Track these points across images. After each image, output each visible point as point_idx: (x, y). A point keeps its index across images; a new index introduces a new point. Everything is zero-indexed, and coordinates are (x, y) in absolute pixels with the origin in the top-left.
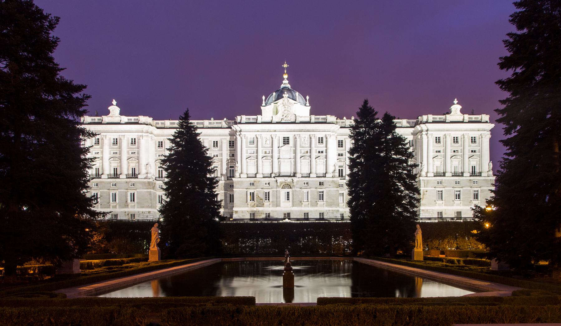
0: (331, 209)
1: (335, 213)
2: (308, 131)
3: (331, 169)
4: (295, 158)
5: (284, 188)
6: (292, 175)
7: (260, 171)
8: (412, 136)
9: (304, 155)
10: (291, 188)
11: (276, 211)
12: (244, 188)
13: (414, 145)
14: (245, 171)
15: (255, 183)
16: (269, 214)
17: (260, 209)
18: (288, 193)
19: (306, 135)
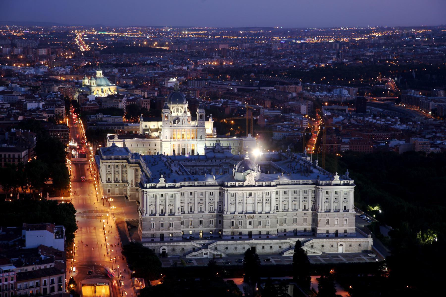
0: (272, 229)
3: (273, 208)
4: (254, 203)
7: (237, 211)
11: (245, 231)
14: (229, 211)
17: (237, 230)
18: (251, 221)
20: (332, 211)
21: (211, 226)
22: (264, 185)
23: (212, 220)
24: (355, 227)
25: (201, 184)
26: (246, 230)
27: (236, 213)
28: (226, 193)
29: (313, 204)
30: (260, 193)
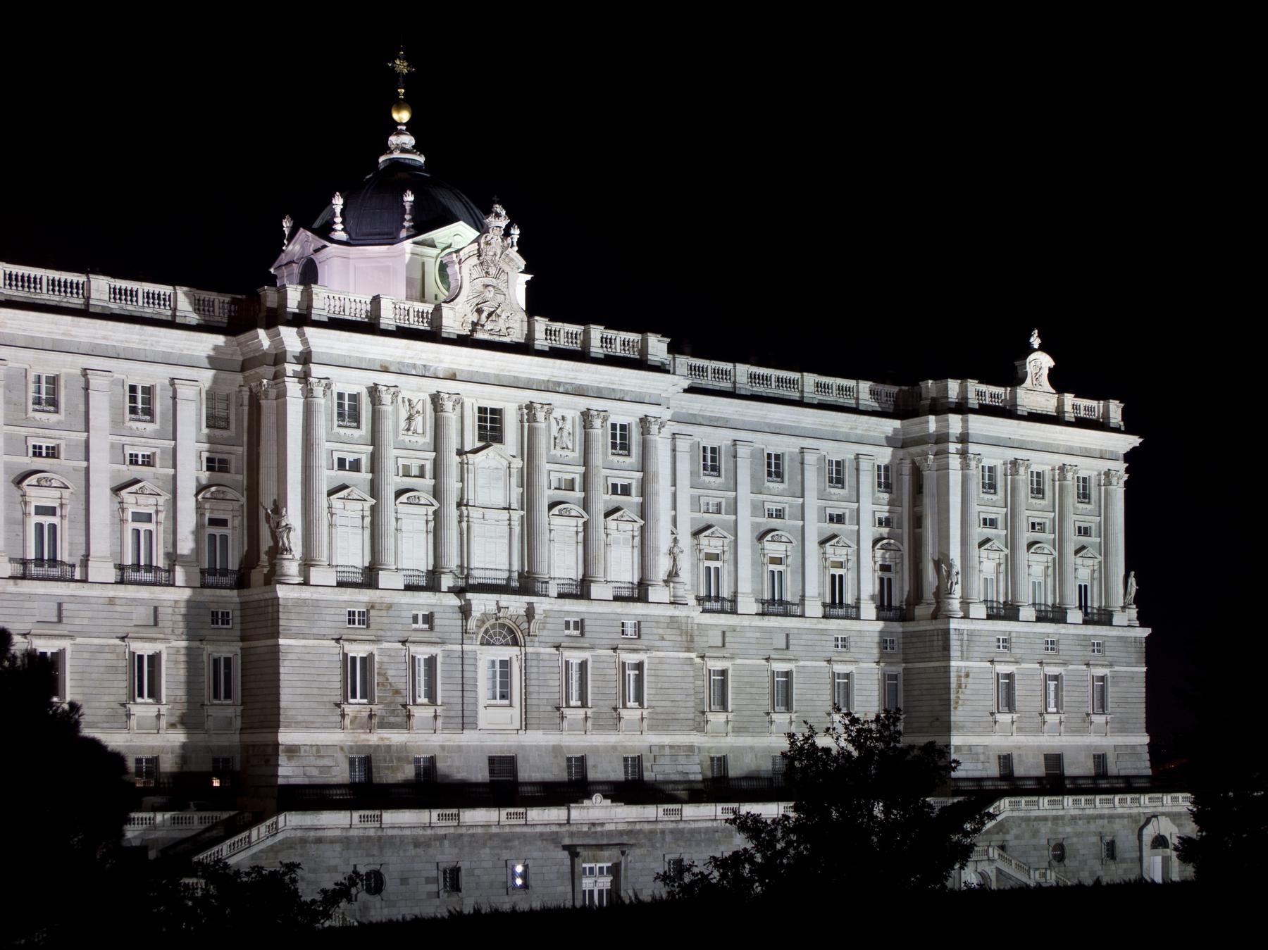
0: (666, 740)
1: (682, 760)
2: (580, 392)
4: (528, 503)
5: (488, 644)
6: (515, 584)
8: (891, 449)
9: (561, 495)
10: (515, 642)
11: (459, 749)
12: (323, 637)
13: (894, 487)
15: (372, 613)
16: (432, 760)
17: (396, 737)
18: (505, 664)
19: (569, 407)
20: (1027, 613)
21: (143, 709)
22: (596, 349)
23: (154, 659)
24: (1145, 739)
25: (55, 299)
26: (468, 738)
27: (384, 579)
28: (293, 389)
29: (885, 568)
30: (568, 426)
